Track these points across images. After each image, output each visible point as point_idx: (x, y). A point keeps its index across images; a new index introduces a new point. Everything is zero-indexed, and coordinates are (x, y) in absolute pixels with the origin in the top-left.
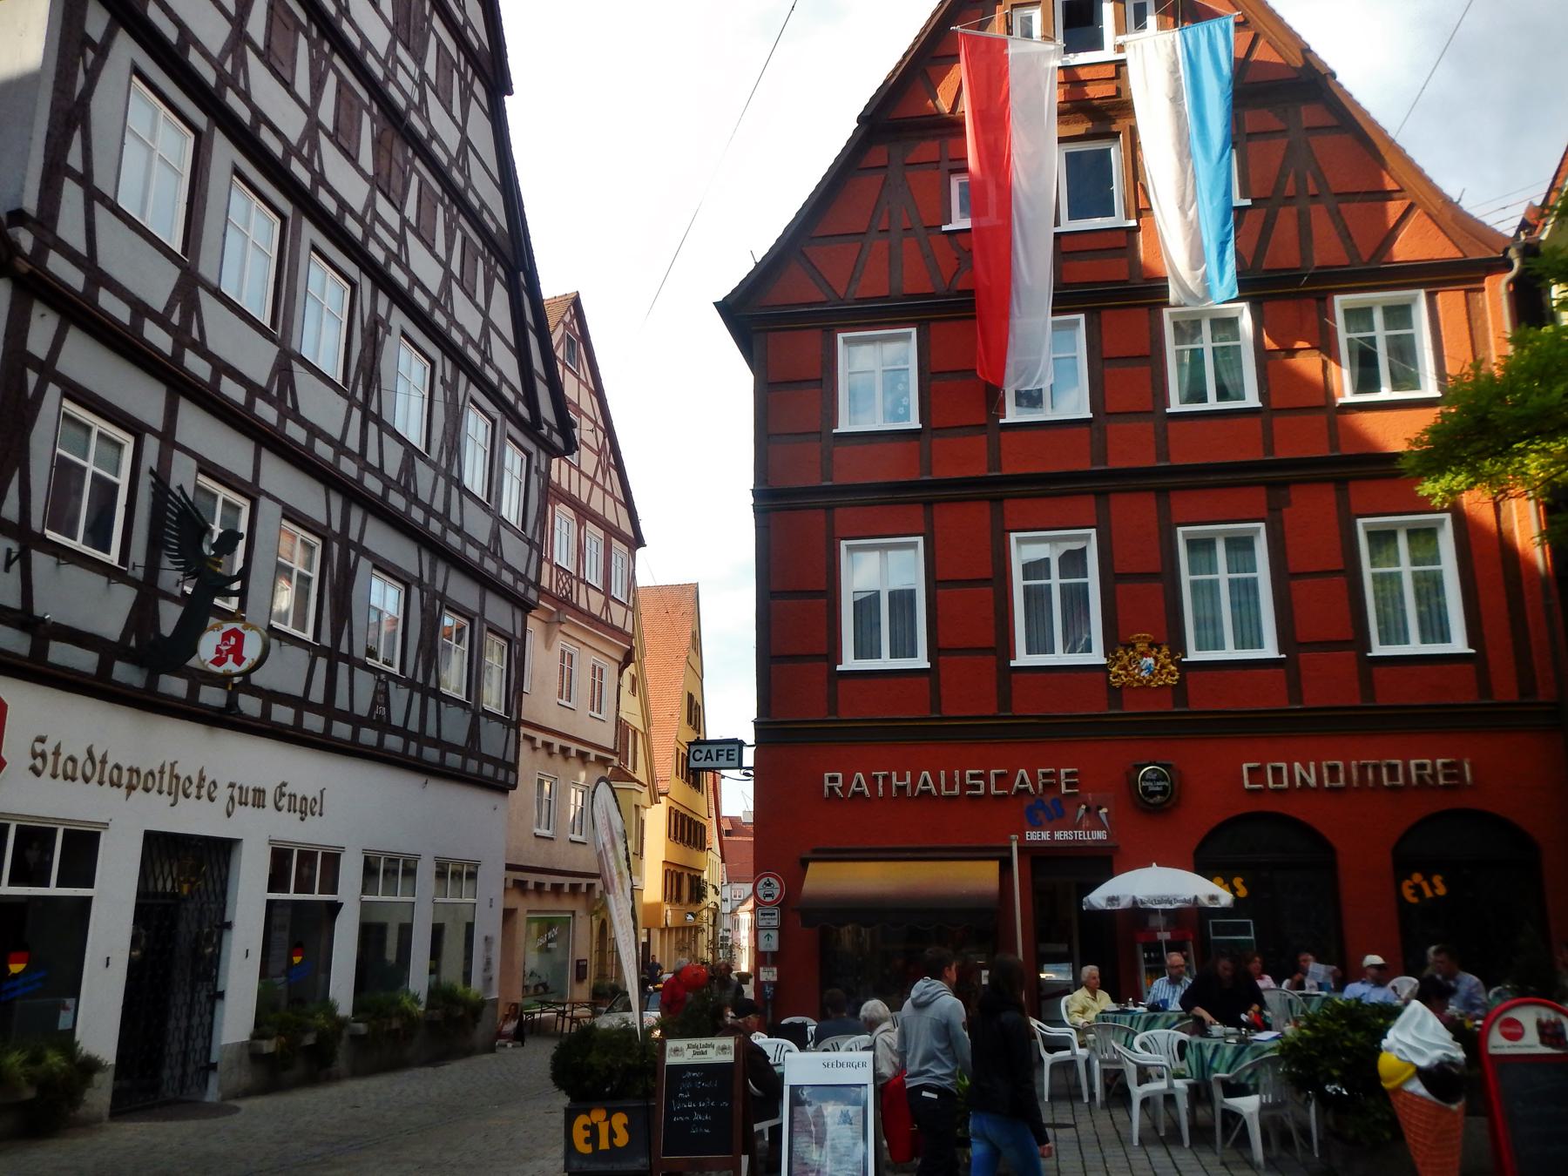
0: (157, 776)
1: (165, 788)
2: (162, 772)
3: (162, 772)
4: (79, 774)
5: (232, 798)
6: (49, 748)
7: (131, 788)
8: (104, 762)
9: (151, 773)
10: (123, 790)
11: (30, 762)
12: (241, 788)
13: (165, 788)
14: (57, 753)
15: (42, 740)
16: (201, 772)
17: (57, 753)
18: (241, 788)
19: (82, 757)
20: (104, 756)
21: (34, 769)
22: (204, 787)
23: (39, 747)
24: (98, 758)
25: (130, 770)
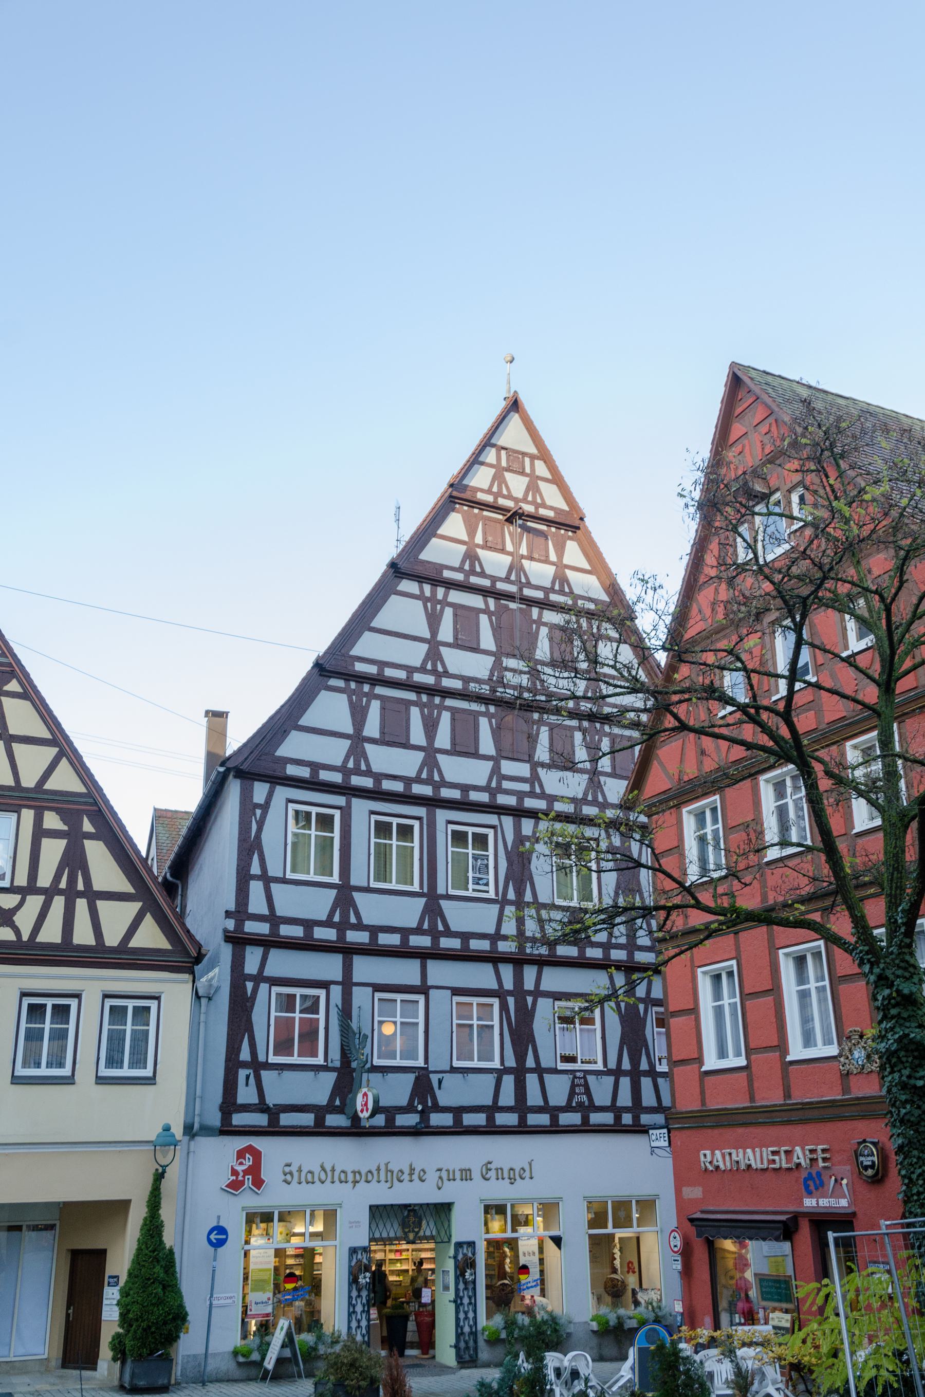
0: (375, 1173)
1: (383, 1178)
2: (378, 1169)
3: (378, 1169)
4: (316, 1179)
5: (440, 1178)
6: (294, 1168)
7: (355, 1182)
8: (333, 1170)
9: (370, 1172)
10: (350, 1185)
11: (283, 1177)
12: (448, 1171)
13: (383, 1178)
14: (300, 1170)
15: (289, 1165)
16: (411, 1166)
17: (300, 1170)
18: (448, 1171)
19: (317, 1170)
20: (333, 1167)
21: (285, 1181)
22: (415, 1174)
23: (287, 1169)
24: (328, 1168)
25: (354, 1172)
